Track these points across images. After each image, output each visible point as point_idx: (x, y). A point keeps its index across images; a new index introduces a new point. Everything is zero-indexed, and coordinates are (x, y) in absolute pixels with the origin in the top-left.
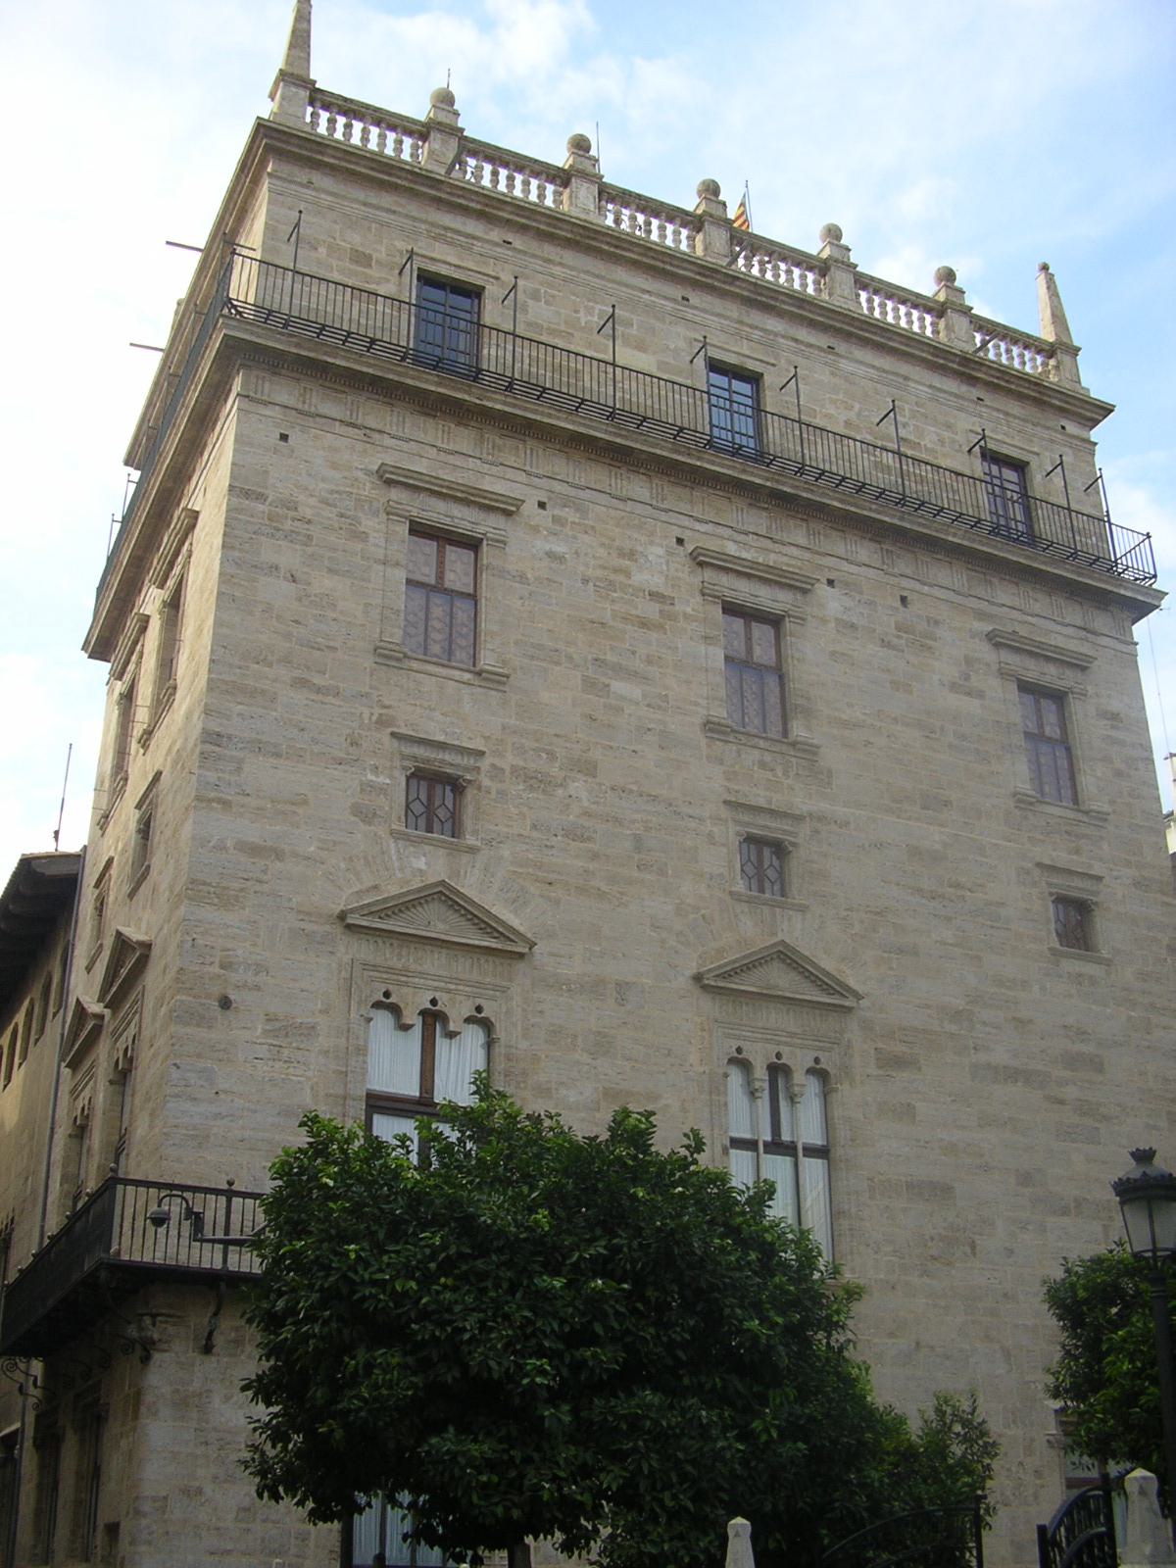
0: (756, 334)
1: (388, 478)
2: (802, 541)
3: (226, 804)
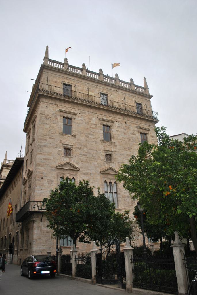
0: (107, 89)
1: (60, 111)
2: (113, 116)
3: (41, 154)
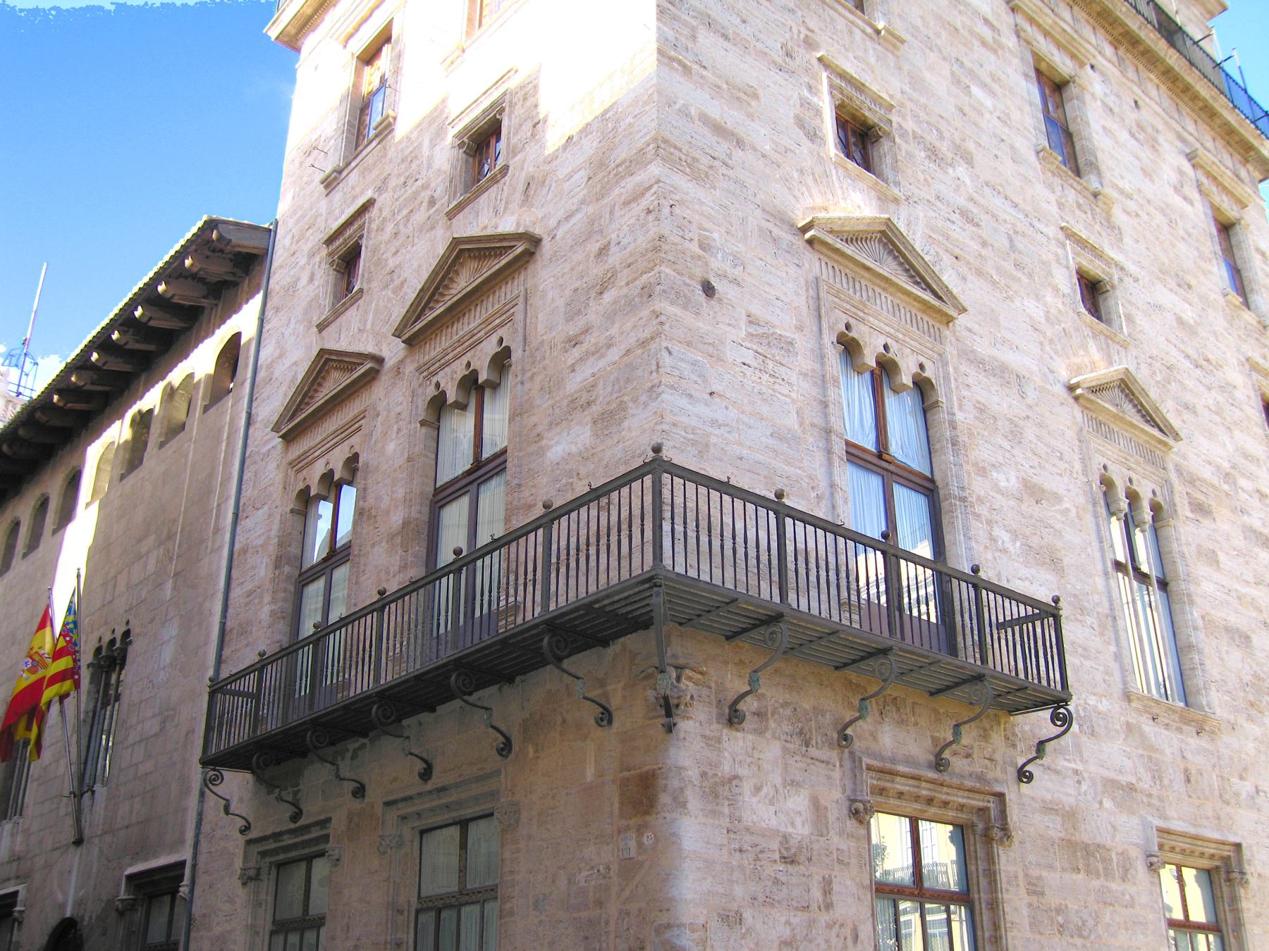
3: (687, 70)
